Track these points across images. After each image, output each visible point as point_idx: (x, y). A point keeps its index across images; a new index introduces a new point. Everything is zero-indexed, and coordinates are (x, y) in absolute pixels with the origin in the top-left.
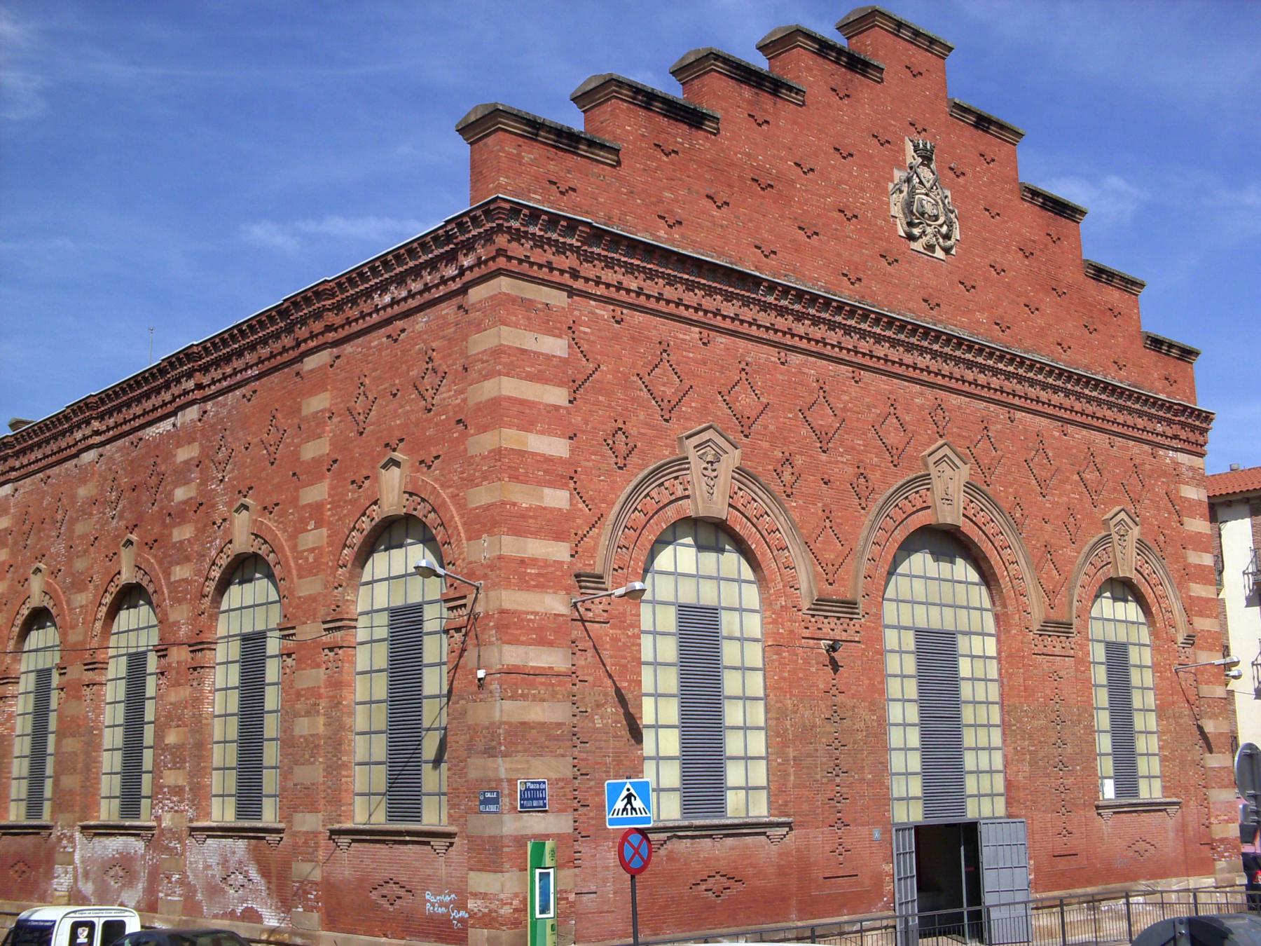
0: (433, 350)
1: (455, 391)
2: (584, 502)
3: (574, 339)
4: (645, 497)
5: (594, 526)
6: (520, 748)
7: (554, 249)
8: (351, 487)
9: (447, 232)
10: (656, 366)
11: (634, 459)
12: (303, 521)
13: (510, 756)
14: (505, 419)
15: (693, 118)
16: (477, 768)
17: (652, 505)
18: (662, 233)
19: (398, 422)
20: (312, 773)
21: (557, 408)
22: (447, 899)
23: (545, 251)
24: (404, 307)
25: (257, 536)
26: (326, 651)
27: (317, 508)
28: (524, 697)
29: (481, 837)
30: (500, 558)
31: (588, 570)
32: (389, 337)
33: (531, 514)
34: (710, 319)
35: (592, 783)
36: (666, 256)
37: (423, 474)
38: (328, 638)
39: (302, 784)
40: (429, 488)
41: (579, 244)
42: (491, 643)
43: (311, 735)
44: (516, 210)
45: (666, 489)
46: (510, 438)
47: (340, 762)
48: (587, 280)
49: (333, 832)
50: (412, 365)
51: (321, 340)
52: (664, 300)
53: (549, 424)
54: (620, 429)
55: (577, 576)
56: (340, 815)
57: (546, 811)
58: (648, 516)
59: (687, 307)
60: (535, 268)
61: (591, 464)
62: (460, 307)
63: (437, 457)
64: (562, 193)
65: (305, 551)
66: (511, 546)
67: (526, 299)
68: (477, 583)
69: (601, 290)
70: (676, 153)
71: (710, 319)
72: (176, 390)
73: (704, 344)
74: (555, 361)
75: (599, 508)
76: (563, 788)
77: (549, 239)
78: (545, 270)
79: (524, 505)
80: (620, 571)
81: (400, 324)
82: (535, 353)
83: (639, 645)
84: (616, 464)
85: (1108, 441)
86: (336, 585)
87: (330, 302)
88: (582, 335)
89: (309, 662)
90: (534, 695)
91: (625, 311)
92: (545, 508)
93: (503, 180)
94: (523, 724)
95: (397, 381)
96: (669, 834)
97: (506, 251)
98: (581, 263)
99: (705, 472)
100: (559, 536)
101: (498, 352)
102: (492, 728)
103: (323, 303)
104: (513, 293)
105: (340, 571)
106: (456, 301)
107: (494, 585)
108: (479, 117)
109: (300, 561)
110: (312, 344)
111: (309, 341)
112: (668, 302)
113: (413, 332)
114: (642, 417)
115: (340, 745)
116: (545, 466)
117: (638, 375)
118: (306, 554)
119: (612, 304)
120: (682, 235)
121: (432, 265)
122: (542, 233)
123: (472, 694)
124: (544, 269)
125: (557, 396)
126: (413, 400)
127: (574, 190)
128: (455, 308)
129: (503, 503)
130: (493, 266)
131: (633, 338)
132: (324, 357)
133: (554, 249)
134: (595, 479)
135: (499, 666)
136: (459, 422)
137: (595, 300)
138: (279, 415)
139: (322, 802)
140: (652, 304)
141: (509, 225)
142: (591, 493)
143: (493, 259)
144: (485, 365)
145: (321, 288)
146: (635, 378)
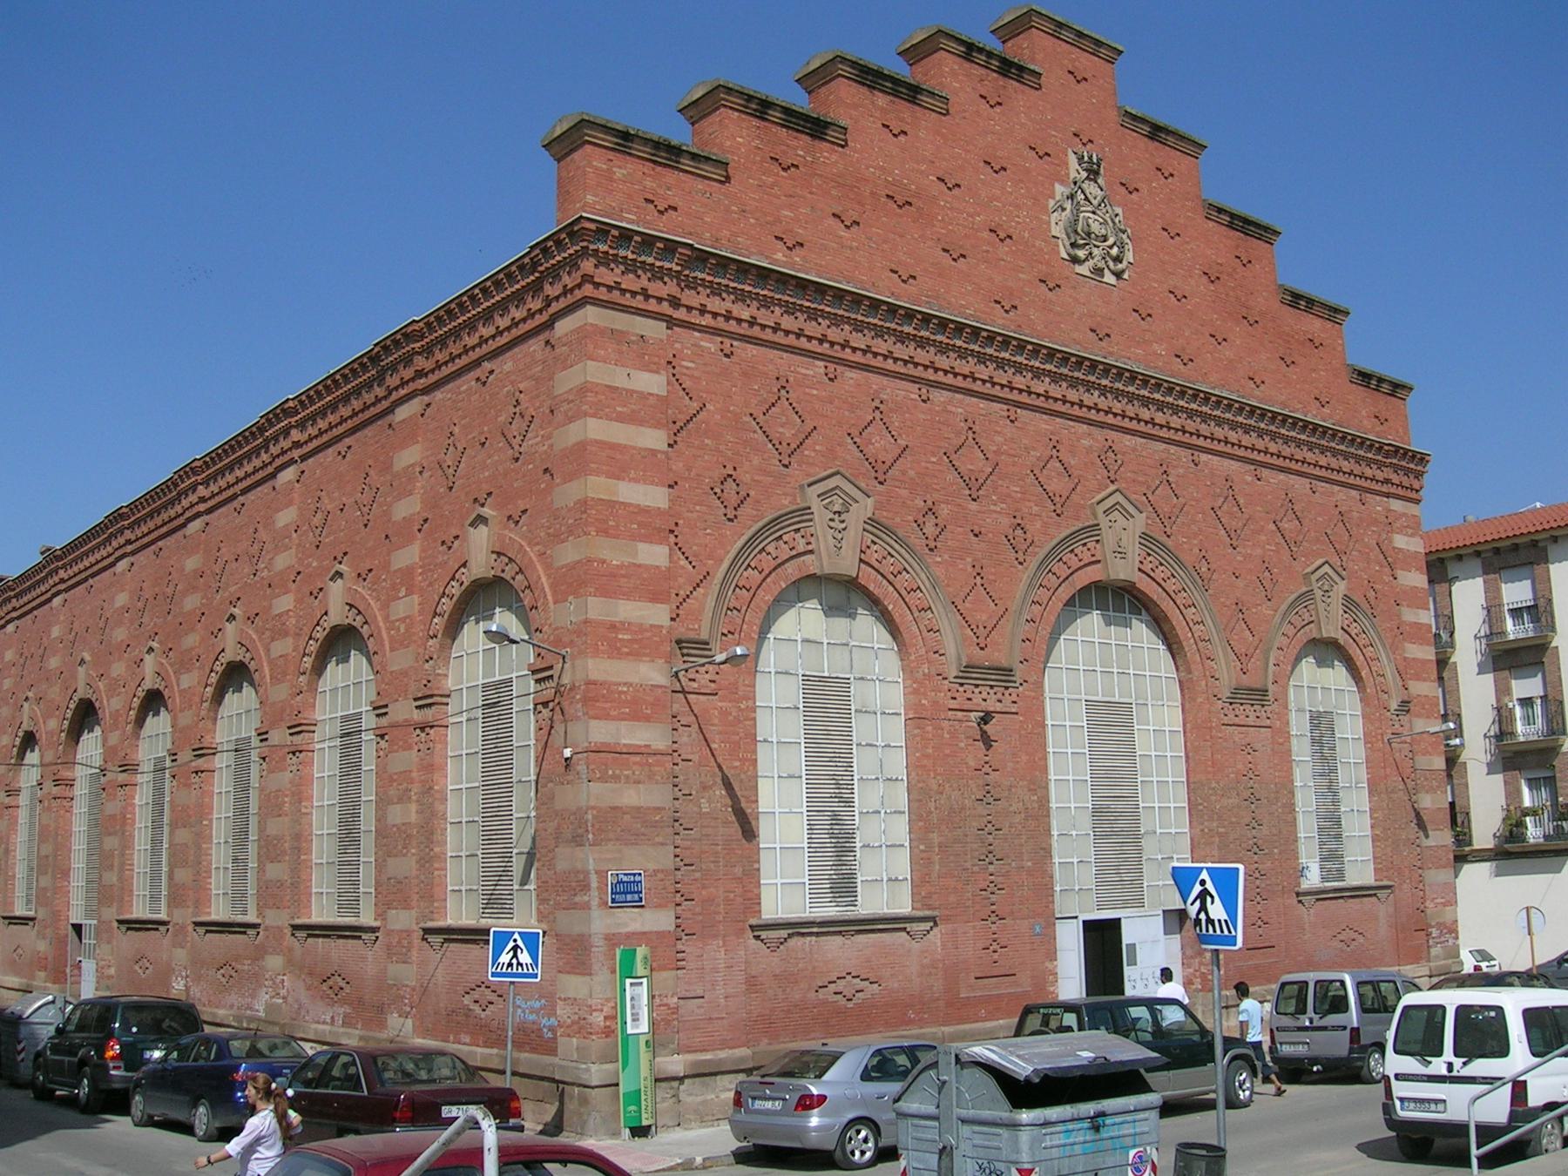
0: (521, 392)
1: (543, 436)
2: (687, 558)
3: (674, 375)
4: (760, 552)
5: (698, 585)
6: (611, 836)
7: (649, 275)
8: (441, 549)
9: (532, 259)
10: (773, 405)
11: (746, 510)
12: (394, 587)
13: (600, 845)
14: (592, 465)
15: (816, 128)
16: (565, 859)
17: (768, 561)
18: (779, 256)
19: (487, 474)
20: (404, 866)
21: (654, 452)
22: (537, 1005)
23: (639, 277)
24: (492, 345)
25: (351, 606)
26: (418, 731)
27: (408, 572)
28: (616, 778)
29: (569, 936)
30: (586, 622)
31: (692, 635)
32: (478, 379)
33: (623, 572)
34: (837, 351)
35: (698, 875)
36: (783, 280)
37: (511, 530)
38: (417, 716)
39: (395, 878)
40: (517, 546)
41: (679, 268)
42: (578, 718)
43: (404, 824)
44: (603, 231)
45: (786, 543)
46: (597, 486)
47: (432, 853)
48: (690, 309)
49: (427, 931)
50: (500, 411)
51: (412, 387)
52: (709, 312)
53: (644, 471)
54: (730, 476)
55: (678, 642)
56: (432, 912)
57: (643, 906)
58: (764, 574)
59: (810, 338)
60: (628, 295)
61: (695, 515)
62: (547, 342)
63: (524, 512)
64: (661, 212)
65: (397, 620)
66: (597, 608)
67: (616, 330)
68: (563, 652)
69: (707, 320)
70: (797, 167)
71: (837, 351)
72: (274, 450)
73: (830, 379)
74: (652, 401)
75: (705, 565)
76: (662, 880)
77: (643, 262)
78: (639, 298)
79: (614, 562)
80: (730, 636)
81: (487, 365)
82: (627, 391)
83: (754, 719)
84: (725, 515)
85: (1191, 458)
86: (427, 657)
87: (419, 345)
88: (685, 371)
89: (401, 743)
90: (627, 777)
91: (735, 343)
92: (640, 566)
93: (590, 199)
94: (615, 808)
95: (486, 429)
96: (790, 931)
97: (592, 277)
98: (682, 290)
99: (832, 524)
100: (655, 598)
101: (583, 390)
102: (579, 814)
103: (412, 346)
104: (601, 324)
105: (431, 642)
106: (543, 337)
107: (580, 653)
108: (564, 129)
109: (392, 632)
110: (402, 392)
111: (400, 390)
112: (787, 333)
113: (501, 373)
114: (756, 461)
115: (432, 834)
116: (639, 518)
117: (751, 415)
118: (397, 624)
119: (720, 335)
120: (804, 258)
121: (518, 297)
122: (634, 256)
123: (558, 776)
124: (638, 297)
125: (654, 439)
126: (501, 448)
127: (675, 209)
128: (543, 343)
129: (589, 561)
130: (578, 294)
131: (745, 374)
132: (414, 406)
133: (649, 275)
134: (701, 533)
135: (586, 744)
136: (546, 470)
137: (699, 331)
138: (372, 473)
139: (416, 897)
140: (768, 335)
141: (595, 247)
142: (695, 548)
143: (579, 286)
144: (571, 405)
145: (410, 329)
146: (749, 419)
